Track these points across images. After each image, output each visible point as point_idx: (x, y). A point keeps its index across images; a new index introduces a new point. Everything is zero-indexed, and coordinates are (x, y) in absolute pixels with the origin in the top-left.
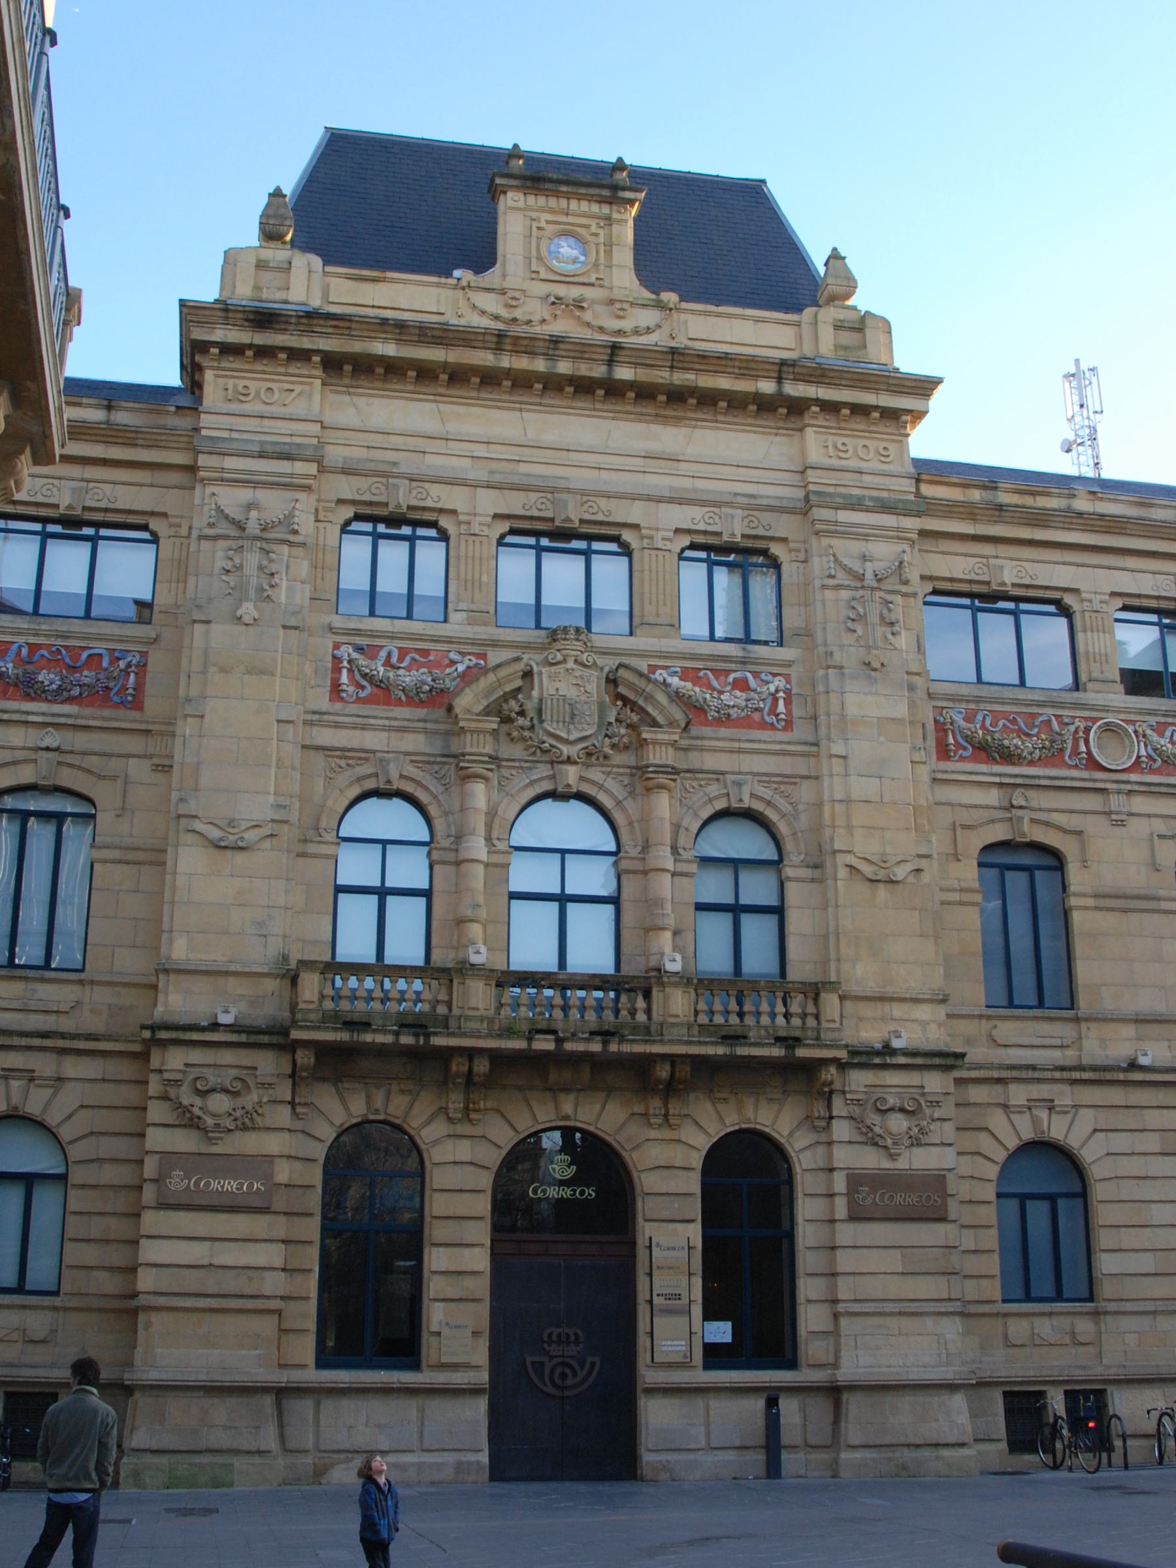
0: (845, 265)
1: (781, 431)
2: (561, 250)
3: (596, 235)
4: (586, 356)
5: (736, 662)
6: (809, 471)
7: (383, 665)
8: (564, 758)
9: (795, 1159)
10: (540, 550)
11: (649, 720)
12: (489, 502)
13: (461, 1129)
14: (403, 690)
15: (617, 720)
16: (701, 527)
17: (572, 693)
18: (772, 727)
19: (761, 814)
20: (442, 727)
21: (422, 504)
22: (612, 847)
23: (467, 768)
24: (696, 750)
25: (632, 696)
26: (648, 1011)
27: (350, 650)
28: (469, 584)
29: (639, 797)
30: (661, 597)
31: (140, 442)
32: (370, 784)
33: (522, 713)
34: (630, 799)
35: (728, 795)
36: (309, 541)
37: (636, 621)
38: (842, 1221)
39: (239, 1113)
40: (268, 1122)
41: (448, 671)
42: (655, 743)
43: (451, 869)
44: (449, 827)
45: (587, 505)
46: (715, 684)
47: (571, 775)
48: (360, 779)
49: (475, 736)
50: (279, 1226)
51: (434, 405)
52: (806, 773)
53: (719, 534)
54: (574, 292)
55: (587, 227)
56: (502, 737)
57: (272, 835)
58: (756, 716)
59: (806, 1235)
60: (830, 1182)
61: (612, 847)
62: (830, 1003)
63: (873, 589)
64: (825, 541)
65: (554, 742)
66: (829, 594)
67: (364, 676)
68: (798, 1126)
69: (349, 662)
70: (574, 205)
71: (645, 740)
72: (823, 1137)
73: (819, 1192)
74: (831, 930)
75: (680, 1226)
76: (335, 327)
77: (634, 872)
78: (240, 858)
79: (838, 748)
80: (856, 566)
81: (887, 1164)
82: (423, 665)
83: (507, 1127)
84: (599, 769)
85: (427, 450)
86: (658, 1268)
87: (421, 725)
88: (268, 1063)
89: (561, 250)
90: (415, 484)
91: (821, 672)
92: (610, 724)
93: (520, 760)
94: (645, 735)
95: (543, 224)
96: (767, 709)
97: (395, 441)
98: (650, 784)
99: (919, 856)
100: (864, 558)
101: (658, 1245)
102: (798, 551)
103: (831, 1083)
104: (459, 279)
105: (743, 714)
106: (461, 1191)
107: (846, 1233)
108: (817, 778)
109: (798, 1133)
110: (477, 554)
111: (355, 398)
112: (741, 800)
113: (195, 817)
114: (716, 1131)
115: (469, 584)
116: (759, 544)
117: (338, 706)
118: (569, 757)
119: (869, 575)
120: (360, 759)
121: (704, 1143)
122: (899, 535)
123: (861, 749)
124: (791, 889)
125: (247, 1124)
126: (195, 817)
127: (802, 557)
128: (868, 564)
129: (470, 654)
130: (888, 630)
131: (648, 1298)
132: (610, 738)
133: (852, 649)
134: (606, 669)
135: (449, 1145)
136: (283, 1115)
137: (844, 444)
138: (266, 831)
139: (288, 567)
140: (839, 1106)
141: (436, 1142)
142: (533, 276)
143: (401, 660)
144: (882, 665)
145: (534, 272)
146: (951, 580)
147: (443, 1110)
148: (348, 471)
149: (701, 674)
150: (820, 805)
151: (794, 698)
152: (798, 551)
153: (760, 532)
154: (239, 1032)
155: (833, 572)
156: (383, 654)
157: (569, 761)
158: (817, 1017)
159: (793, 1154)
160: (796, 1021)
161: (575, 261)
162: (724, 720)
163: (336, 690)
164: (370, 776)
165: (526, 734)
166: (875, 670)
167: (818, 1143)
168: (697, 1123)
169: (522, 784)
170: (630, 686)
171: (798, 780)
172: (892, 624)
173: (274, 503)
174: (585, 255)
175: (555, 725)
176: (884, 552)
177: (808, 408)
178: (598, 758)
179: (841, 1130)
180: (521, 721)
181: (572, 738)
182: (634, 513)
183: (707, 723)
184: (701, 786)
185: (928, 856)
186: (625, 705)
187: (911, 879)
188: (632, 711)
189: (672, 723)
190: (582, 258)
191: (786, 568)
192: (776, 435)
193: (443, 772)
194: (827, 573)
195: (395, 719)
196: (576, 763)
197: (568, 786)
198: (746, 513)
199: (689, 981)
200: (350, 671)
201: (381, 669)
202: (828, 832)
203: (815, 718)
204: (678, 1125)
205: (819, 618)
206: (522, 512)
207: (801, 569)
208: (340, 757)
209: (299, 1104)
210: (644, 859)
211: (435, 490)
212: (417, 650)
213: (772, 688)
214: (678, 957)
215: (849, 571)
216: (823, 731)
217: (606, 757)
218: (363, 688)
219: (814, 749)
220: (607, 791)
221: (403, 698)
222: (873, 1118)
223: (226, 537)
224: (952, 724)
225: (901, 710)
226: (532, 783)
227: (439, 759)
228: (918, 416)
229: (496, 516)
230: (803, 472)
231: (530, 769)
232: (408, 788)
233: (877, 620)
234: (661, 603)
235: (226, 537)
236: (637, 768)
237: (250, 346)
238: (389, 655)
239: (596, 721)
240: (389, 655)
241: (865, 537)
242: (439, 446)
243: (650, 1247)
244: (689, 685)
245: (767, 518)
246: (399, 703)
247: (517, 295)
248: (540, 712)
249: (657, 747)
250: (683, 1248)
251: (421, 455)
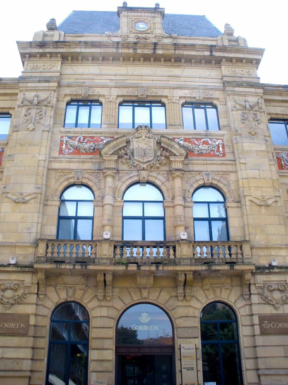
0: (230, 26)
1: (213, 68)
3: (150, 21)
4: (146, 47)
5: (204, 135)
6: (224, 78)
7: (78, 142)
8: (142, 168)
9: (237, 311)
10: (134, 107)
11: (173, 155)
12: (115, 92)
13: (103, 303)
14: (84, 150)
15: (161, 155)
16: (189, 95)
17: (145, 147)
18: (218, 156)
19: (217, 185)
20: (98, 160)
21: (93, 94)
22: (162, 199)
23: (106, 172)
24: (191, 164)
25: (166, 147)
26: (175, 255)
27: (67, 138)
28: (109, 116)
29: (171, 181)
30: (176, 117)
31: (7, 87)
32: (72, 181)
33: (126, 154)
34: (167, 182)
35: (204, 179)
36: (54, 106)
37: (167, 125)
38: (258, 335)
39: (16, 297)
40: (28, 301)
41: (100, 143)
42: (175, 161)
43: (101, 208)
44: (100, 194)
45: (149, 91)
46: (196, 143)
47: (144, 174)
48: (67, 179)
49: (109, 162)
50: (30, 341)
51: (98, 67)
52: (232, 170)
53: (195, 98)
54: (144, 35)
55: (148, 19)
56: (120, 163)
57: (34, 198)
58: (212, 153)
59: (244, 342)
60: (252, 320)
61: (162, 199)
62: (246, 248)
63: (249, 110)
64: (231, 97)
65: (138, 163)
66: (234, 112)
67: (71, 146)
68: (238, 299)
69: (66, 142)
70: (143, 14)
71: (172, 161)
72: (248, 303)
73: (248, 324)
74: (245, 224)
75: (192, 340)
76: (65, 45)
77: (169, 207)
78: (23, 206)
79: (243, 161)
80: (243, 103)
81: (274, 312)
82: (91, 141)
83: (121, 302)
84: (155, 172)
85: (95, 78)
86: (184, 357)
87: (90, 160)
88: (27, 278)
90: (90, 88)
91: (234, 137)
92: (158, 156)
93: (126, 170)
94: (171, 159)
95: (133, 19)
96: (216, 150)
97: (84, 77)
98: (174, 175)
99: (276, 196)
100: (245, 101)
101: (183, 348)
102: (223, 102)
103: (249, 280)
104: (107, 34)
105: (207, 152)
106: (103, 328)
107: (260, 340)
108: (236, 172)
109: (238, 301)
110: (111, 107)
111: (72, 67)
112: (208, 180)
113: (8, 193)
114: (205, 302)
115: (109, 116)
116: (209, 101)
117: (62, 156)
118: (144, 168)
119: (248, 106)
120: (69, 172)
121: (201, 306)
122: (256, 95)
123: (251, 161)
124: (230, 212)
125: (19, 301)
126: (8, 193)
127: (224, 103)
128: (247, 103)
129: (108, 137)
130: (256, 123)
131: (180, 370)
132: (159, 161)
133: (244, 129)
134: (157, 139)
135: (98, 310)
136: (33, 298)
137: (234, 70)
138: (33, 196)
139: (45, 113)
140: (253, 289)
141: (93, 309)
142: (130, 32)
143: (84, 140)
144: (255, 133)
145: (131, 31)
146: (277, 114)
147: (96, 296)
148: (68, 86)
149: (191, 140)
150: (238, 181)
151: (225, 146)
152: (223, 102)
153: (209, 96)
154: (18, 267)
155: (235, 105)
156: (78, 138)
157: (144, 169)
158: (242, 254)
159: (236, 310)
160: (234, 256)
161: (144, 28)
162: (201, 154)
163: (61, 152)
164: (72, 178)
165: (128, 161)
166: (253, 135)
167: (246, 305)
168: (197, 299)
169: (127, 178)
170: (165, 143)
171: (229, 173)
172: (257, 121)
173: (43, 95)
174: (147, 26)
175: (138, 157)
176: (253, 100)
177: (222, 61)
178: (154, 168)
179: (255, 299)
180: (126, 156)
181: (144, 161)
182: (166, 92)
183: (195, 156)
184: (193, 176)
185: (280, 197)
186: (163, 150)
187: (274, 205)
188: (166, 152)
189: (181, 155)
190: (146, 27)
191: (219, 108)
192: (212, 69)
193: (98, 175)
194: (233, 106)
195: (81, 158)
196: (147, 170)
197: (144, 178)
198: (204, 91)
199: (190, 242)
200: (66, 145)
201: (77, 143)
202: (241, 189)
203: (233, 152)
204: (190, 300)
205: (232, 120)
206: (127, 94)
207: (224, 107)
208: (61, 172)
209: (40, 294)
210: (173, 202)
211: (97, 90)
212: (90, 137)
213: (217, 143)
214: (186, 234)
215: (241, 105)
216: (236, 156)
217: (158, 168)
218: (70, 150)
219: (234, 162)
220: (158, 179)
221: (84, 152)
222: (267, 293)
223: (26, 106)
224: (282, 158)
225: (264, 148)
226: (130, 178)
227: (97, 171)
228: (258, 62)
229: (118, 96)
230: (222, 79)
231: (130, 173)
232: (85, 181)
233: (252, 120)
234: (176, 119)
235: (26, 106)
236: (169, 171)
237: (39, 53)
238: (80, 139)
239: (153, 155)
240: (80, 139)
241: (245, 95)
242: (100, 77)
243: (180, 349)
244: (187, 143)
245: (211, 92)
246: (83, 154)
248: (133, 154)
249: (176, 163)
250: (193, 349)
251: (93, 80)
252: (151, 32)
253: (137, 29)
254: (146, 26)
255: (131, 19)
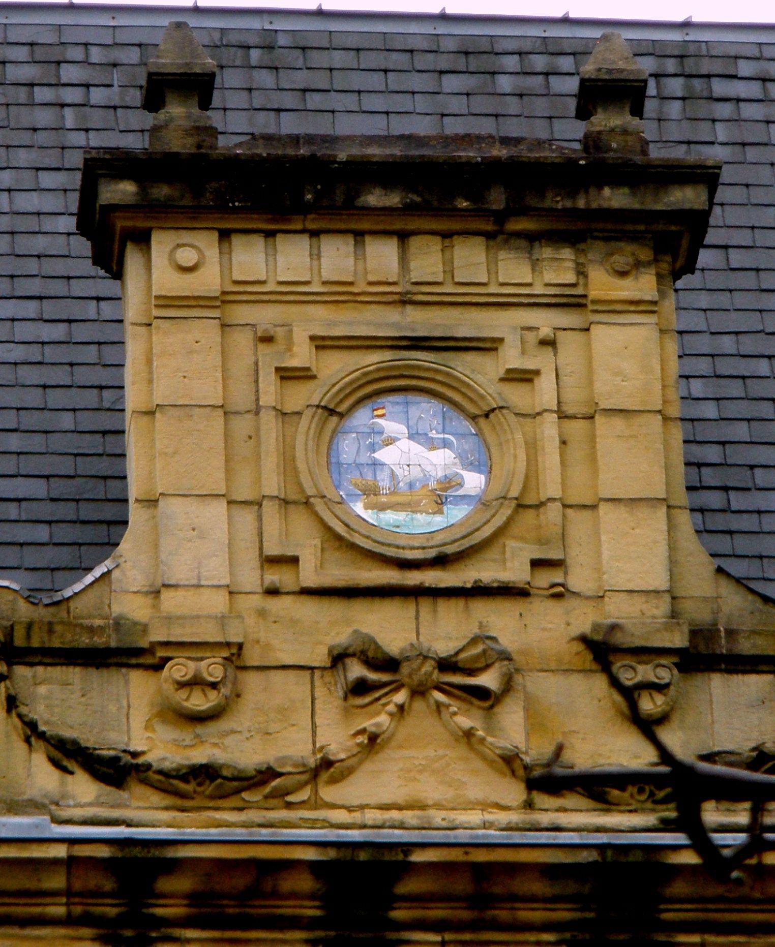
2: (384, 455)
3: (525, 377)
89: (384, 455)
142: (274, 577)
190: (474, 482)
247: (212, 668)
252: (536, 564)
253: (359, 508)
254: (471, 466)
255: (268, 339)
